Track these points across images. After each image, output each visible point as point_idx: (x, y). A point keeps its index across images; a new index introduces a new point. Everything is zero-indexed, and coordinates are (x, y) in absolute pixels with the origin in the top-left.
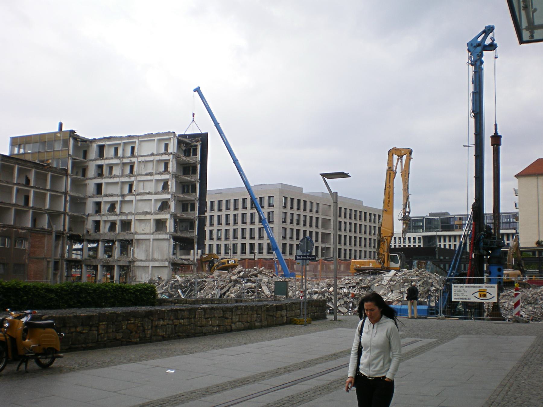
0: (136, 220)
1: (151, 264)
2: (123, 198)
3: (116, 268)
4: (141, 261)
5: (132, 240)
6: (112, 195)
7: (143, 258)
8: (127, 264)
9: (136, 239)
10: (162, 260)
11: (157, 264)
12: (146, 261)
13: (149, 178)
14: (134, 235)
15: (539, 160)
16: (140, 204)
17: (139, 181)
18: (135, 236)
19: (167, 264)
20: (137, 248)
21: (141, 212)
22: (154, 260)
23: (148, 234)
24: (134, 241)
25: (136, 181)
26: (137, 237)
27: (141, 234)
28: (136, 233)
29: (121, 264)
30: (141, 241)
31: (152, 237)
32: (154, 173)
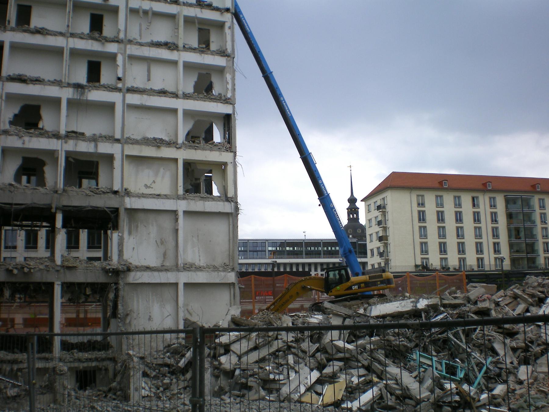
0: (128, 157)
1: (183, 278)
2: (82, 94)
3: (58, 290)
4: (148, 268)
5: (116, 211)
6: (37, 81)
7: (153, 262)
8: (101, 279)
9: (126, 209)
10: (215, 269)
11: (201, 277)
12: (162, 269)
13: (164, 54)
14: (123, 196)
15: (394, 173)
16: (132, 118)
17: (132, 58)
18: (127, 200)
19: (232, 277)
20: (130, 233)
21: (139, 138)
22: (189, 267)
23: (166, 197)
24: (122, 213)
25: (124, 54)
26: (130, 203)
27: (144, 196)
28: (127, 193)
29: (79, 277)
30: (141, 215)
31: (182, 206)
32: (181, 45)
